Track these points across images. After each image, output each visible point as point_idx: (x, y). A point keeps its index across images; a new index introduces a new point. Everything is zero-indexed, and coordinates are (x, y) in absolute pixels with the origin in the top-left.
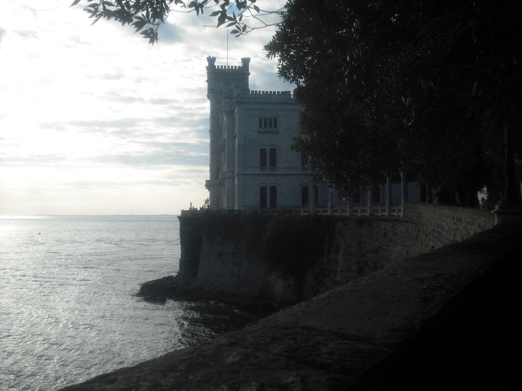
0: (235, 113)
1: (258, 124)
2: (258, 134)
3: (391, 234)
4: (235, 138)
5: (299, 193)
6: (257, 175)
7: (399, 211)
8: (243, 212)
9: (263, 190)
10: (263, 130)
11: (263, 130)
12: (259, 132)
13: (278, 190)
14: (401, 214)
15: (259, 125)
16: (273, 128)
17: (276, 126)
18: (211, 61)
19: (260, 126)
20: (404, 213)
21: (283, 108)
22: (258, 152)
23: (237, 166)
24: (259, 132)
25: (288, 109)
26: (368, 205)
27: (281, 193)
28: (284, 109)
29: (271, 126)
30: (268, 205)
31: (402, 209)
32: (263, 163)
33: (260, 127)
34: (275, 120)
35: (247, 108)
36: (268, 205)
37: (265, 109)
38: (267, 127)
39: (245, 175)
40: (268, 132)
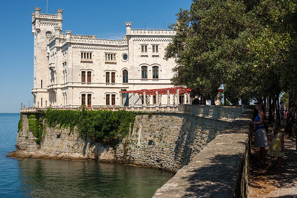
2: (81, 62)
3: (170, 120)
9: (83, 95)
11: (84, 60)
12: (82, 62)
13: (92, 96)
19: (82, 57)
34: (91, 54)
40: (86, 62)
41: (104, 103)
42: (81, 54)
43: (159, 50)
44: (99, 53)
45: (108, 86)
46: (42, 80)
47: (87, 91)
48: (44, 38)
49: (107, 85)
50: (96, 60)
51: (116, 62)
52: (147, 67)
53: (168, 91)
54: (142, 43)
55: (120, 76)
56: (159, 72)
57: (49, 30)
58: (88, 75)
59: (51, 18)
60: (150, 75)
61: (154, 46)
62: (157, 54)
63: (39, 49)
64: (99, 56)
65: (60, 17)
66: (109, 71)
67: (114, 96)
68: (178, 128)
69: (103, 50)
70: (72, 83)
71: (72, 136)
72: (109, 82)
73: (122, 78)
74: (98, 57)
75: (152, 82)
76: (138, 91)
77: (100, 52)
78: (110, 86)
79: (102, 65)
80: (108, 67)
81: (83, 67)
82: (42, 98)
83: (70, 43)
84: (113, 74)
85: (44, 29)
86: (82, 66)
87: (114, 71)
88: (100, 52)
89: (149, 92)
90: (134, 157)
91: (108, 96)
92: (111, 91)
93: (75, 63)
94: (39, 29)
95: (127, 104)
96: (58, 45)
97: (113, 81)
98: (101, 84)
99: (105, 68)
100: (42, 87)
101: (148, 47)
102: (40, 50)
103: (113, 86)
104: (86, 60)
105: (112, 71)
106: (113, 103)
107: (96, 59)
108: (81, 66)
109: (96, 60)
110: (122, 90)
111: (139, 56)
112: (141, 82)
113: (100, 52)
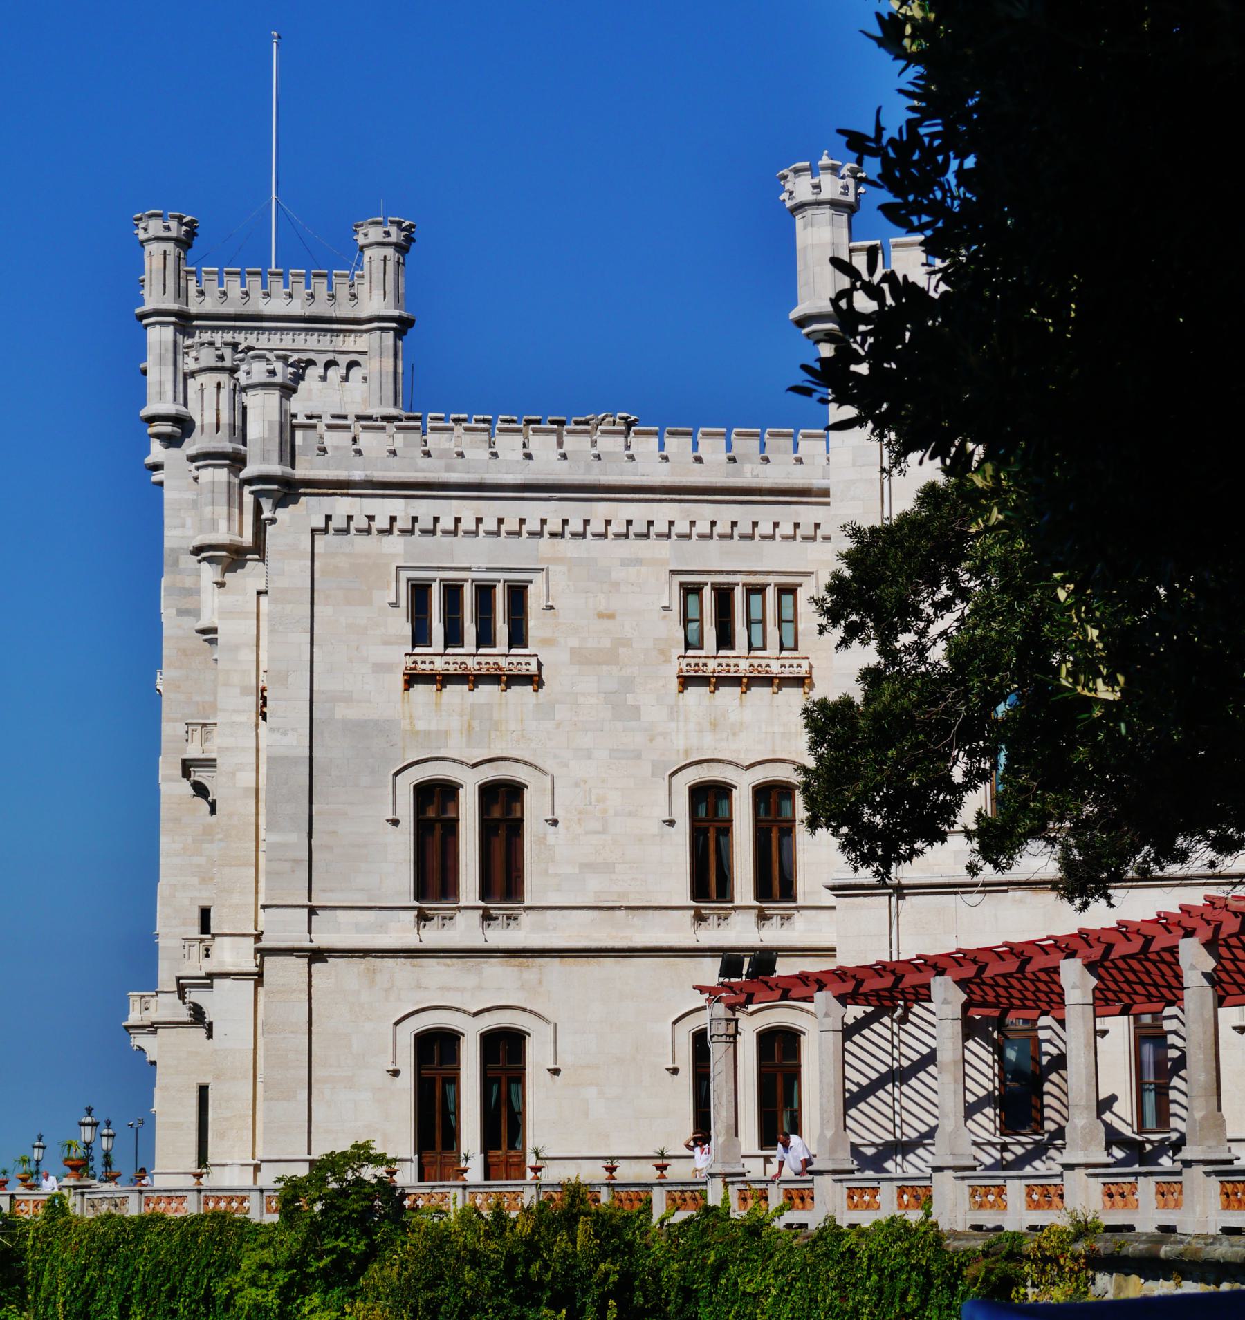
10: (437, 660)
11: (439, 665)
12: (413, 679)
13: (536, 1056)
15: (407, 629)
17: (518, 637)
19: (420, 636)
27: (556, 1072)
28: (575, 525)
29: (485, 638)
34: (517, 594)
39: (317, 955)
42: (404, 601)
44: (615, 585)
50: (582, 658)
59: (297, 307)
64: (611, 616)
65: (378, 293)
72: (724, 890)
74: (607, 624)
77: (625, 563)
79: (653, 713)
80: (714, 725)
81: (428, 734)
82: (203, 1090)
86: (421, 725)
88: (625, 563)
93: (347, 698)
96: (223, 524)
98: (637, 918)
99: (680, 743)
104: (468, 656)
107: (574, 642)
108: (405, 724)
109: (582, 658)
113: (618, 574)
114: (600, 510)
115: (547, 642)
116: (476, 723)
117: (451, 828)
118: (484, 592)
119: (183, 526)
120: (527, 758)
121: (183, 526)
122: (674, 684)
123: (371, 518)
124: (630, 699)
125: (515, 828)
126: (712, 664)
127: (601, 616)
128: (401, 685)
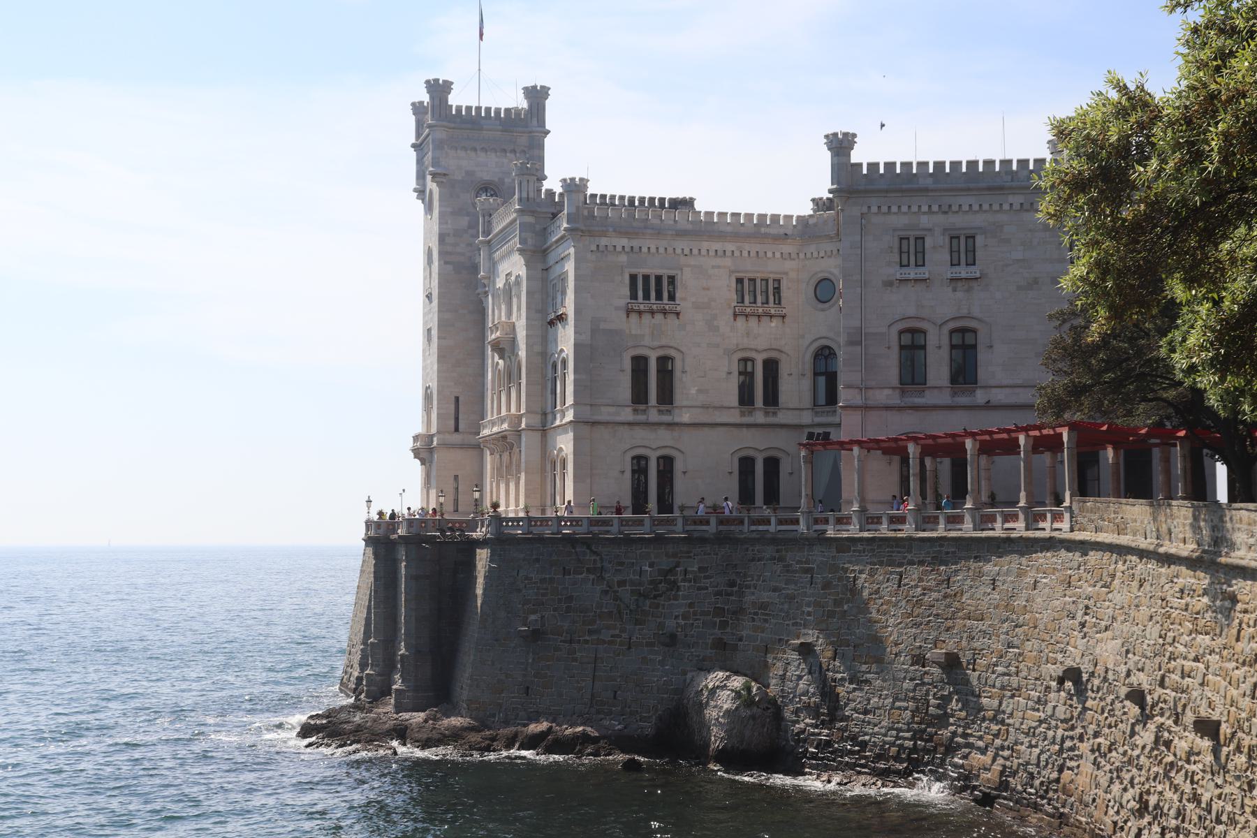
0: (552, 258)
1: (626, 291)
2: (628, 317)
4: (551, 323)
5: (731, 473)
6: (623, 424)
7: (1057, 517)
8: (539, 523)
11: (642, 307)
12: (629, 312)
13: (678, 466)
14: (1065, 525)
15: (629, 293)
16: (665, 301)
17: (672, 297)
18: (439, 89)
19: (634, 296)
20: (1071, 521)
21: (691, 250)
22: (628, 365)
23: (570, 400)
24: (629, 312)
25: (704, 252)
26: (968, 506)
27: (684, 473)
28: (695, 251)
29: (659, 296)
30: (652, 504)
31: (1067, 516)
32: (639, 396)
33: (631, 299)
34: (672, 280)
35: (598, 246)
36: (652, 504)
37: (645, 250)
38: (649, 299)
39: (594, 423)
40: (652, 313)
41: (727, 494)
43: (979, 254)
45: (747, 420)
46: (457, 399)
47: (654, 443)
48: (468, 214)
49: (742, 414)
51: (784, 311)
52: (924, 332)
53: (1022, 439)
54: (900, 221)
55: (804, 375)
56: (982, 356)
57: (485, 176)
58: (658, 371)
60: (938, 367)
61: (958, 238)
62: (975, 271)
63: (446, 263)
64: (708, 289)
66: (753, 355)
67: (772, 465)
68: (1072, 608)
69: (728, 262)
70: (591, 405)
71: (586, 642)
73: (806, 384)
75: (945, 398)
76: (890, 440)
77: (713, 267)
78: (759, 418)
80: (748, 334)
83: (582, 231)
84: (771, 367)
85: (468, 173)
86: (634, 332)
87: (773, 355)
88: (713, 267)
89: (933, 447)
90: (867, 738)
91: (746, 465)
92: (758, 443)
94: (445, 175)
95: (829, 499)
97: (772, 398)
100: (457, 430)
101: (929, 242)
102: (450, 267)
103: (771, 420)
105: (765, 356)
106: (772, 496)
108: (627, 331)
110: (810, 436)
111: (889, 284)
112: (895, 400)
114: (705, 245)
115: (683, 299)
116: (655, 332)
117: (645, 372)
118: (659, 279)
119: (447, 223)
120: (675, 345)
121: (447, 223)
122: (732, 318)
123: (615, 246)
124: (715, 323)
125: (671, 373)
126: (748, 310)
127: (704, 289)
128: (625, 316)
